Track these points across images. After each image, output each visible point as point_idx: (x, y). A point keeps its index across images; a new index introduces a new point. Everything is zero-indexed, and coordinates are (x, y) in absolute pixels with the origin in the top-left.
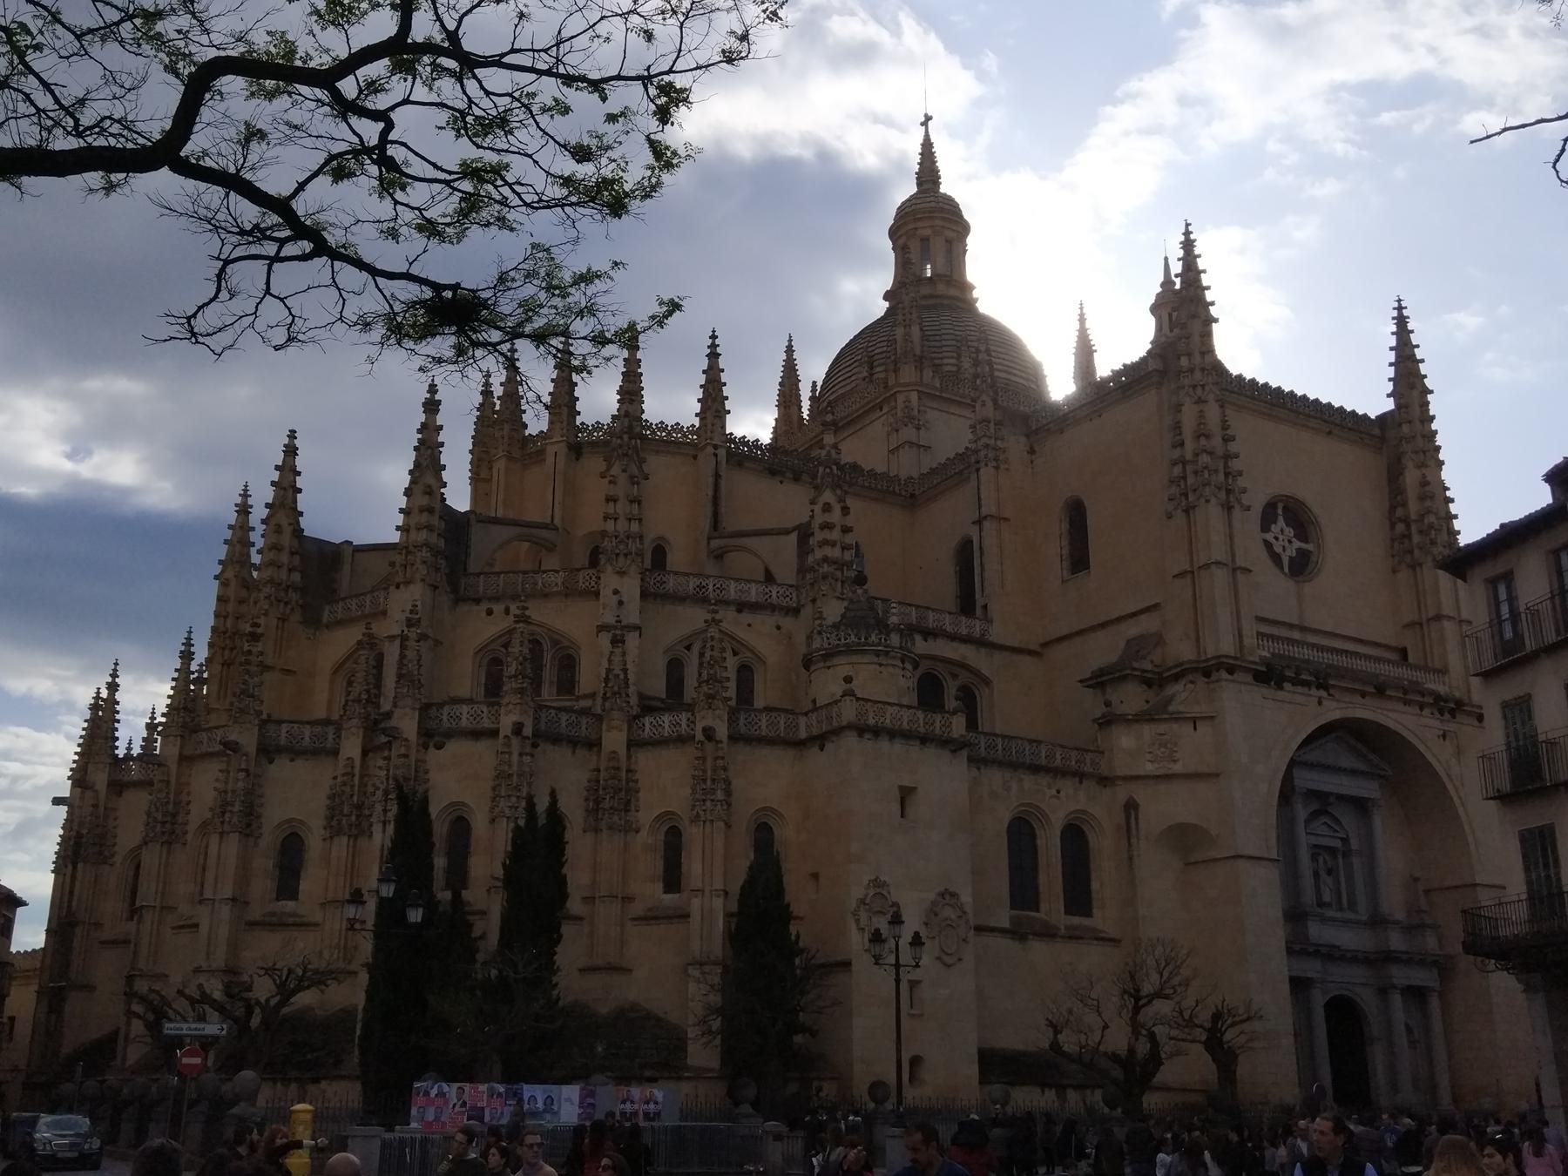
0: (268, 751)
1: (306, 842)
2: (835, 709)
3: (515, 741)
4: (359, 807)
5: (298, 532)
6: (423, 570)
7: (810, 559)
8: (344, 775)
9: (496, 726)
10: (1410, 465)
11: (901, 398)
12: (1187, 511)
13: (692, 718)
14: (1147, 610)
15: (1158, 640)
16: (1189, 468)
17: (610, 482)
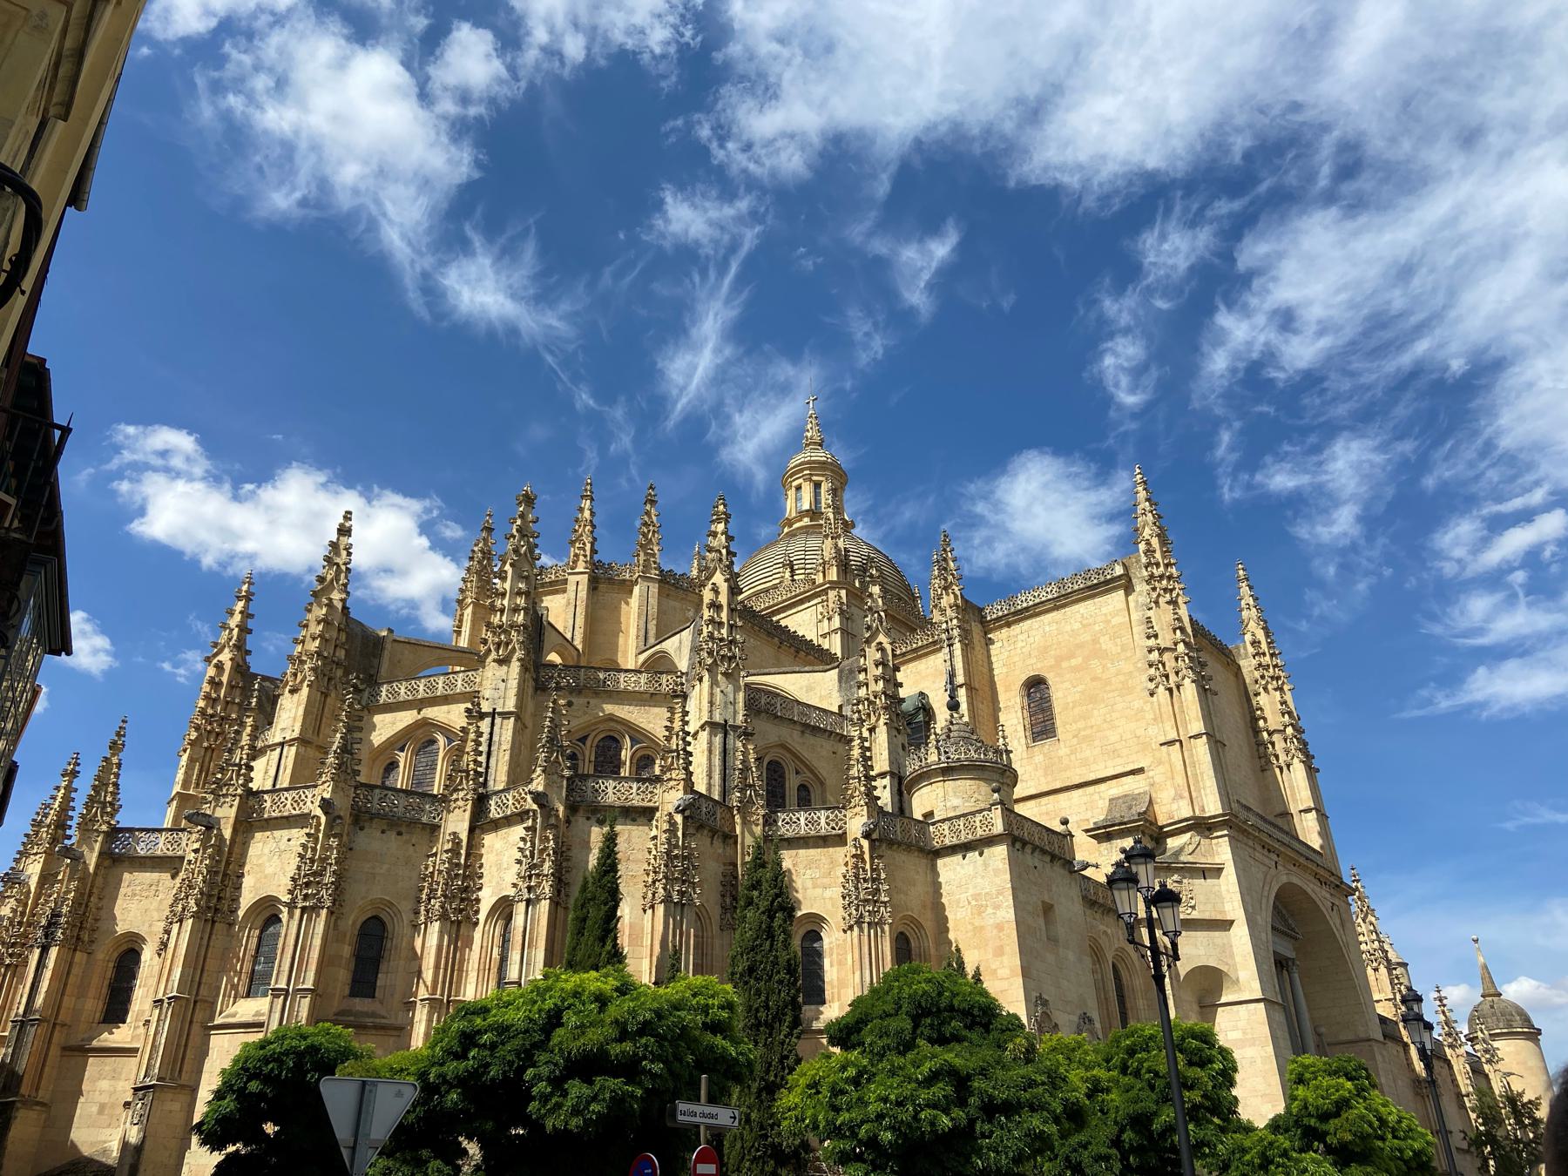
0: (360, 818)
1: (389, 927)
2: (979, 817)
3: (679, 818)
4: (466, 889)
5: (345, 608)
6: (519, 654)
7: (862, 692)
8: (447, 852)
9: (651, 804)
10: (1270, 687)
11: (832, 594)
12: (1170, 690)
13: (832, 816)
14: (1133, 772)
15: (1151, 802)
16: (1167, 657)
17: (713, 589)
